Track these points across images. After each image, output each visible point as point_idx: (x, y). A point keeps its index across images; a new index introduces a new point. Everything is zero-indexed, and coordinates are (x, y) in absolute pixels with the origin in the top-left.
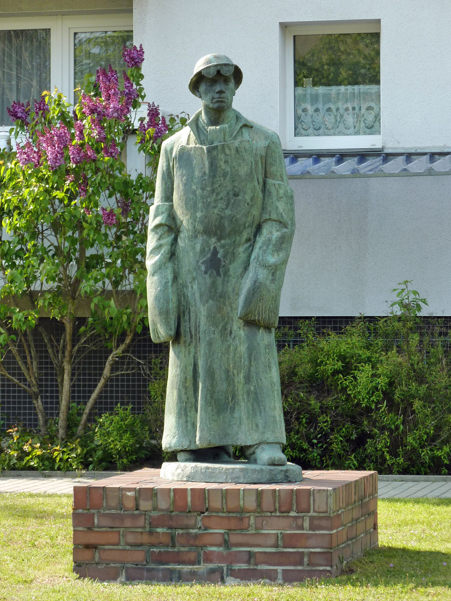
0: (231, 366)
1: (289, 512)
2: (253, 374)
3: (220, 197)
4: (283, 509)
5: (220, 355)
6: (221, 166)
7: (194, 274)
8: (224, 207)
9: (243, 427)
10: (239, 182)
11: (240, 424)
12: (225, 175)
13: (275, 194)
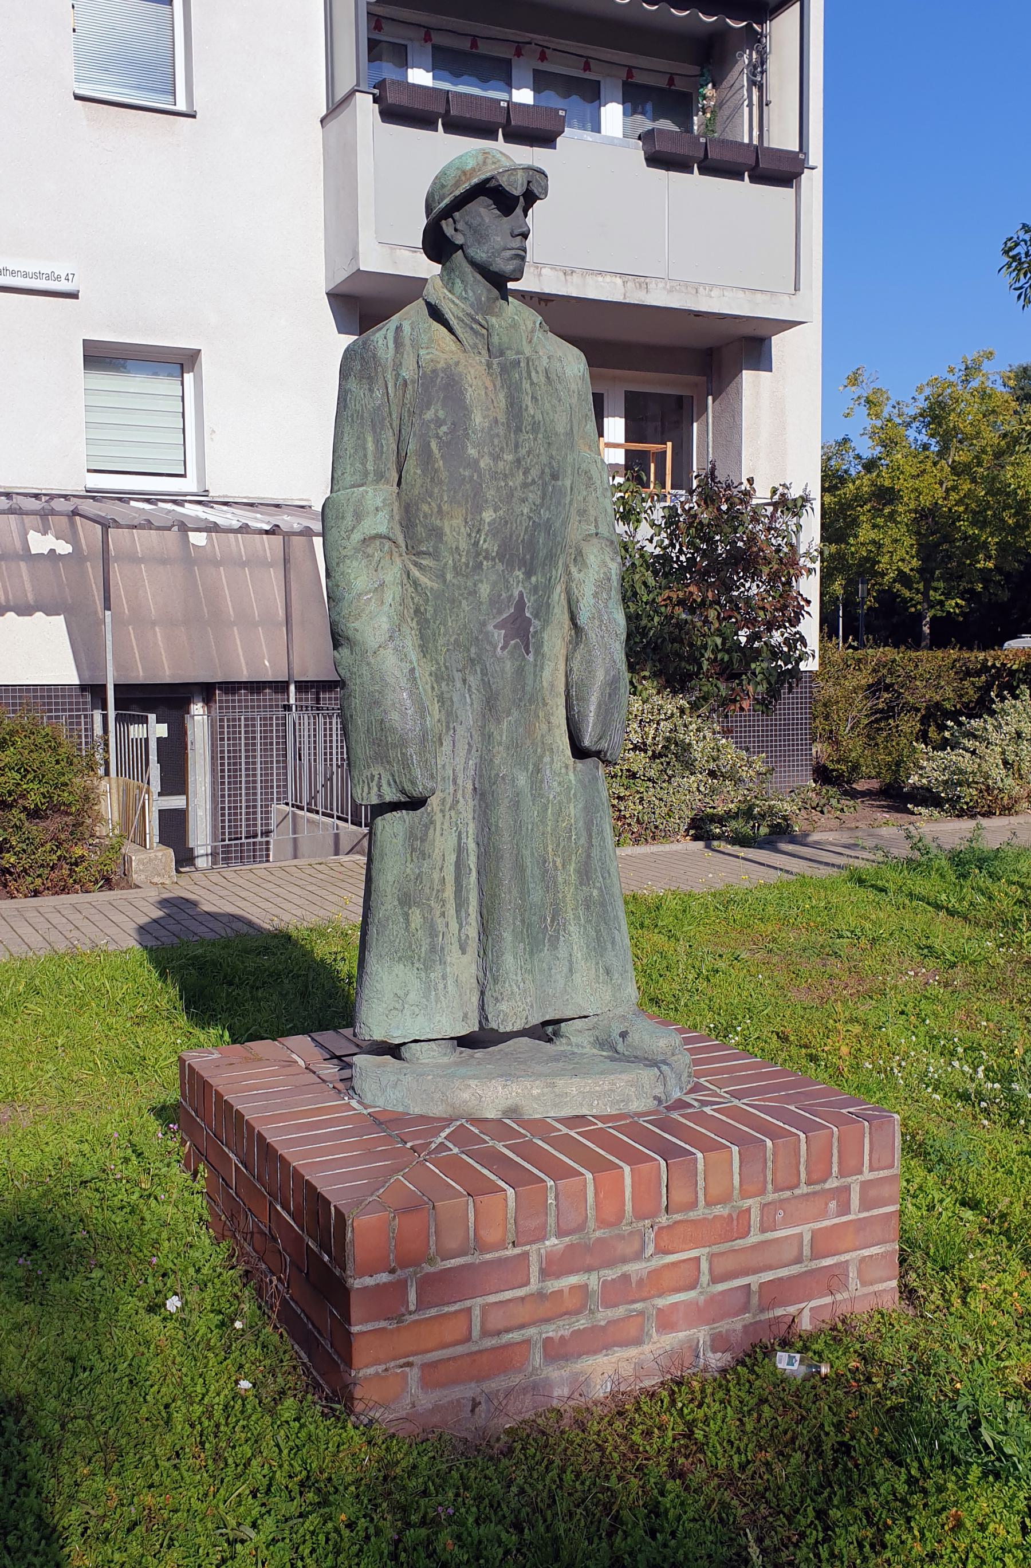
1: (825, 1181)
2: (596, 863)
3: (529, 480)
4: (815, 1177)
7: (473, 650)
8: (538, 502)
9: (577, 978)
11: (571, 970)
12: (535, 427)
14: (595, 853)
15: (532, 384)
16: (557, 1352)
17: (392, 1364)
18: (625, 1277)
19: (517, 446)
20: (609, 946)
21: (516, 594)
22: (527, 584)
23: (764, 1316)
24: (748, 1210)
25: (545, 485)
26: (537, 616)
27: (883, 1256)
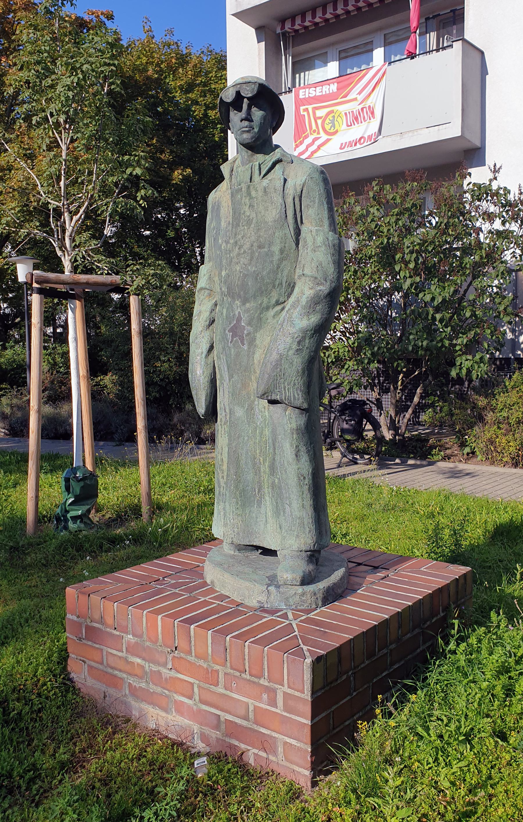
0: (258, 452)
5: (246, 438)
6: (245, 212)
9: (268, 525)
10: (265, 231)
12: (249, 222)
13: (311, 243)
14: (277, 458)
15: (251, 198)
16: (134, 691)
17: (79, 658)
18: (159, 673)
19: (236, 235)
20: (282, 513)
21: (237, 313)
22: (243, 308)
23: (227, 740)
24: (217, 671)
25: (253, 253)
26: (249, 324)
27: (299, 749)
